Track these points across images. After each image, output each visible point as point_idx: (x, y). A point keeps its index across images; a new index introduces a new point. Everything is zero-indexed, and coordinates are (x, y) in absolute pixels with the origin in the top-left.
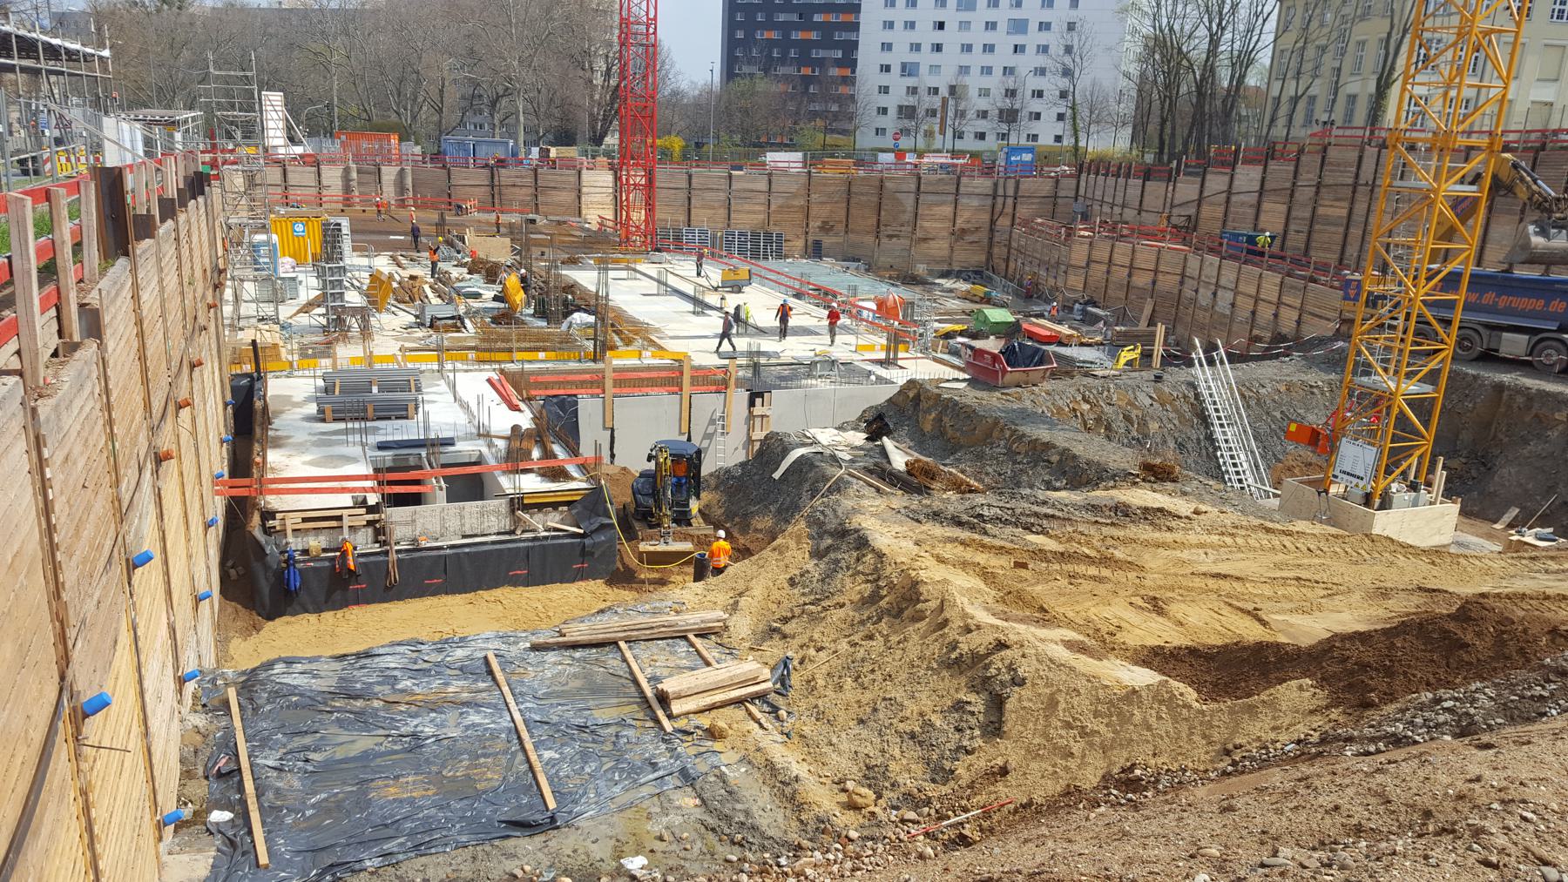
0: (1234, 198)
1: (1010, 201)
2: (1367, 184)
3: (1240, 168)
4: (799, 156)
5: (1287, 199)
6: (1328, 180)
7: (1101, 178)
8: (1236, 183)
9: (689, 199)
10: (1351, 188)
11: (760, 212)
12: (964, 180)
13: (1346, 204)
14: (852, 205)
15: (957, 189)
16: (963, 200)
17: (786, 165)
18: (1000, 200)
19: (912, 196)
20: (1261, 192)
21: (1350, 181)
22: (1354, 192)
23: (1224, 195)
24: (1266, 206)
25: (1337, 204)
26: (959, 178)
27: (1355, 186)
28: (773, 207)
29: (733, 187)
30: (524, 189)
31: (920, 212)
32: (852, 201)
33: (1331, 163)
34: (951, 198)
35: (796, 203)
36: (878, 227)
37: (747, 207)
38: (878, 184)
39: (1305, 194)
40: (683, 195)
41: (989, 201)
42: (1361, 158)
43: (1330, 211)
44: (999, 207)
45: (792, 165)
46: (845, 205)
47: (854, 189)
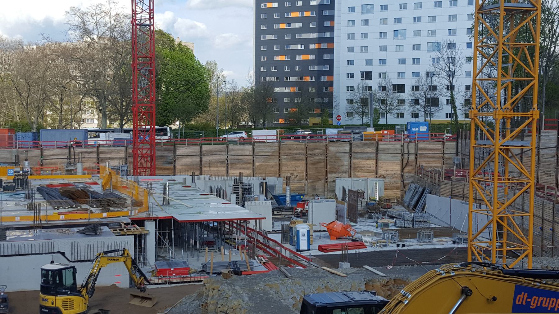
4: (274, 132)
7: (463, 141)
9: (201, 161)
11: (248, 168)
14: (308, 162)
17: (265, 138)
28: (257, 164)
30: (90, 159)
31: (353, 165)
32: (308, 160)
36: (326, 175)
37: (239, 165)
38: (324, 148)
40: (197, 159)
45: (268, 138)
46: (304, 162)
47: (309, 152)
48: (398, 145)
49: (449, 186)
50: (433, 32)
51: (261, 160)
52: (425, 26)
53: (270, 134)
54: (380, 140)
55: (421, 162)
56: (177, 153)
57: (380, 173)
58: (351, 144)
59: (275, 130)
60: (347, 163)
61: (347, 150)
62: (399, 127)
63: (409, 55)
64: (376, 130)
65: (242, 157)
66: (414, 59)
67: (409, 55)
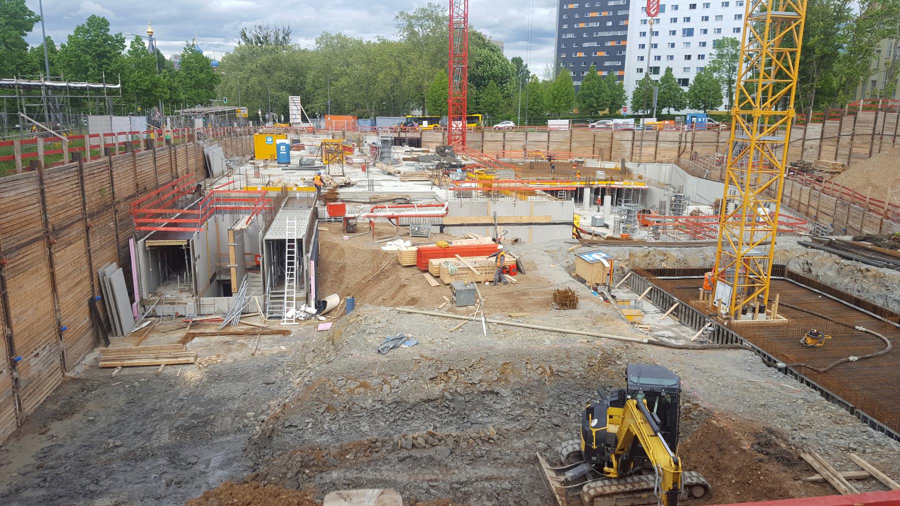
0: (807, 143)
1: (689, 145)
2: (879, 134)
3: (810, 125)
5: (835, 143)
6: (858, 131)
8: (807, 133)
10: (871, 137)
12: (661, 133)
13: (868, 146)
15: (657, 138)
16: (661, 145)
18: (683, 144)
19: (630, 143)
20: (822, 139)
21: (870, 132)
22: (873, 139)
23: (801, 141)
24: (824, 147)
25: (864, 146)
26: (658, 132)
27: (873, 135)
29: (528, 140)
33: (859, 122)
34: (654, 143)
35: (564, 147)
39: (845, 141)
41: (677, 145)
42: (876, 118)
43: (860, 150)
44: (682, 150)
48: (677, 134)
49: (719, 171)
50: (719, 30)
51: (554, 146)
52: (711, 25)
53: (563, 124)
54: (661, 129)
55: (697, 149)
56: (485, 139)
57: (658, 159)
58: (634, 133)
59: (568, 121)
60: (629, 151)
61: (631, 138)
62: (679, 118)
63: (695, 51)
64: (658, 120)
65: (537, 143)
66: (699, 56)
67: (695, 51)
